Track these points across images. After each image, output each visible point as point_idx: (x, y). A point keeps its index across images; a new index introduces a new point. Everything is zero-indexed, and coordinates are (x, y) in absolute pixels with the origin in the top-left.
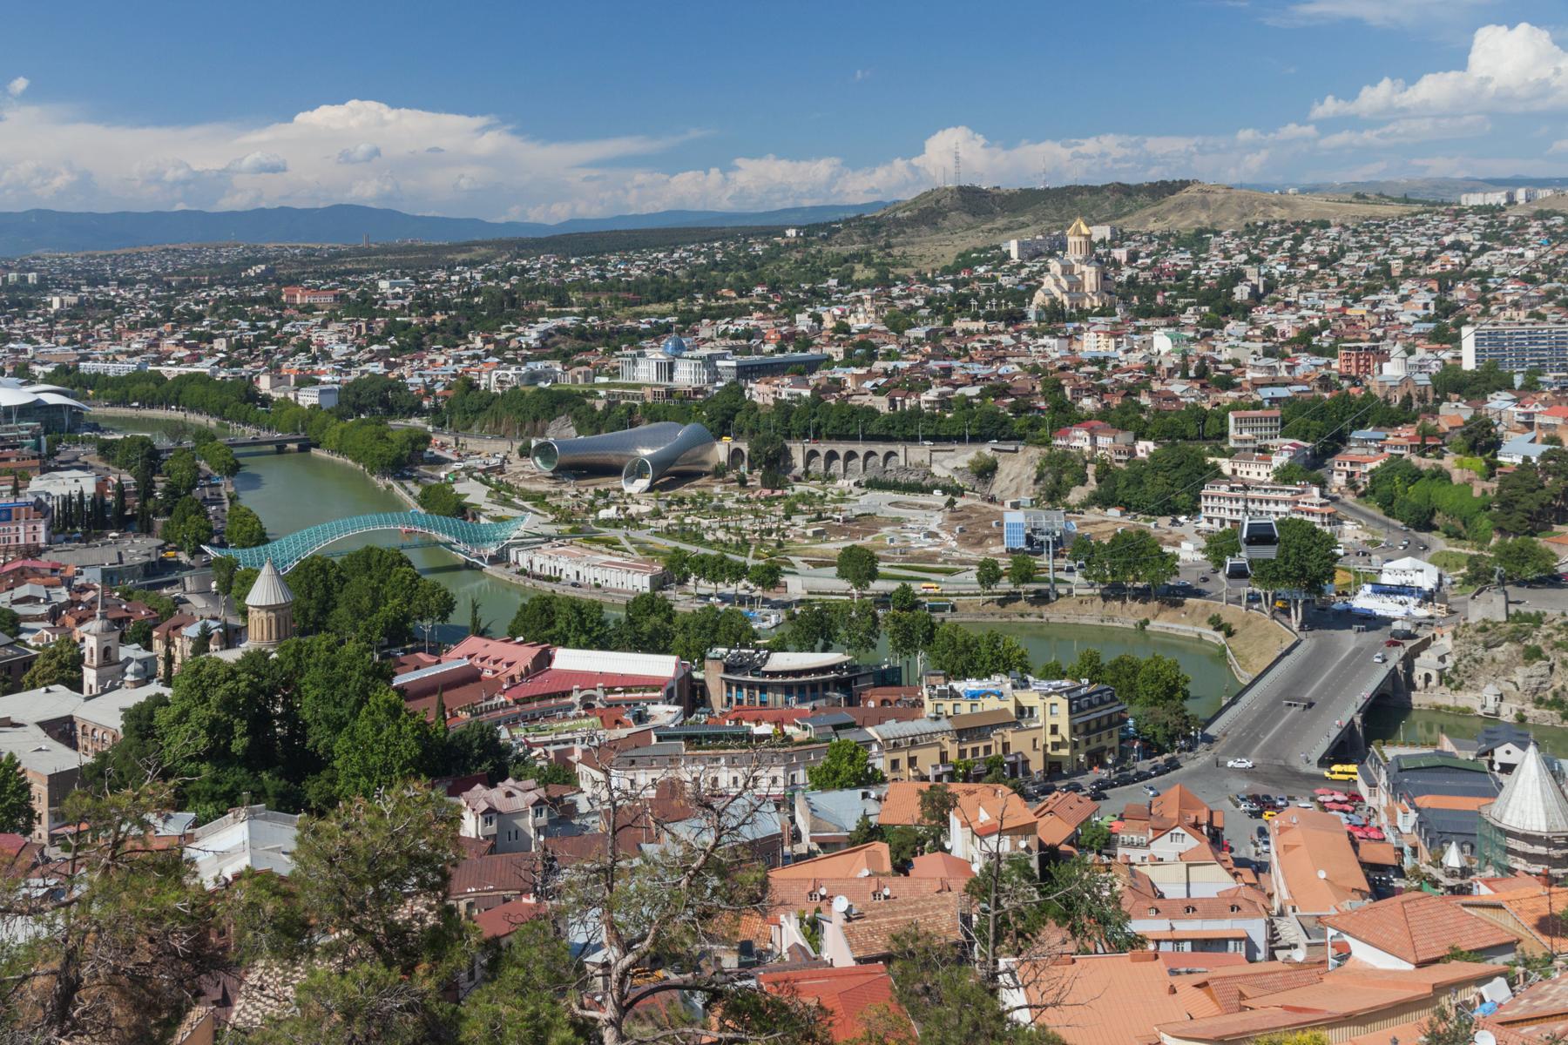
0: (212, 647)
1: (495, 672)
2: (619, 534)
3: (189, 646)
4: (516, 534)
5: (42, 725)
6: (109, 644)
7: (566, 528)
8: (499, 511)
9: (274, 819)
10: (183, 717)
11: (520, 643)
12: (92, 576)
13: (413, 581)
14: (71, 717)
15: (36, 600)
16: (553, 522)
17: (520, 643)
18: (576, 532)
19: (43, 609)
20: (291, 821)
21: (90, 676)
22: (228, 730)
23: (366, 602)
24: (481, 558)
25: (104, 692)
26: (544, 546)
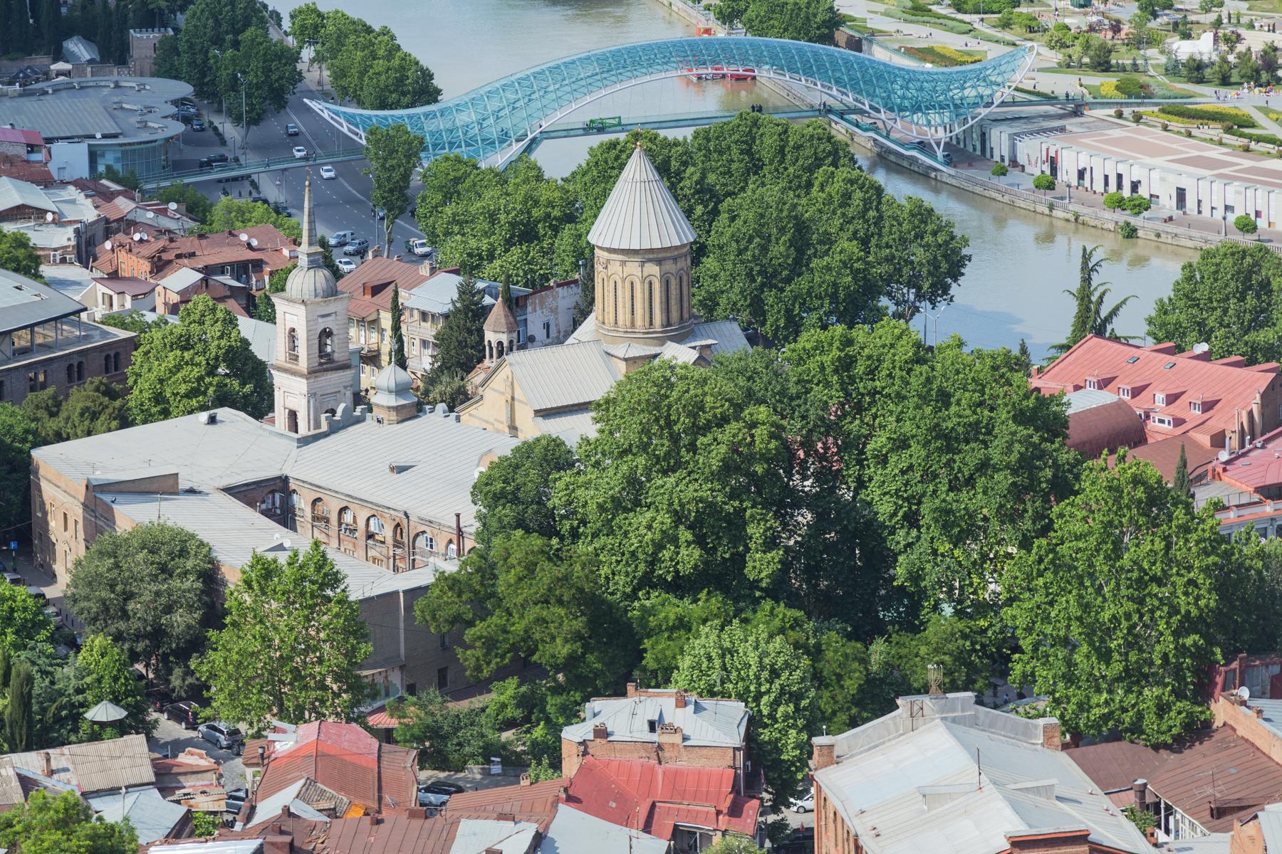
0: (491, 336)
1: (1178, 422)
2: (1245, 100)
3: (429, 331)
4: (1006, 93)
5: (229, 490)
6: (329, 323)
7: (1107, 83)
8: (920, 34)
9: (992, 726)
10: (633, 496)
11: (1205, 357)
12: (70, 158)
13: (867, 203)
14: (284, 480)
15: (41, 213)
16: (1067, 66)
17: (1205, 357)
18: (1136, 91)
19: (63, 237)
20: (1027, 734)
21: (291, 392)
22: (736, 524)
23: (779, 249)
24: (923, 146)
25: (334, 428)
26: (1070, 123)
